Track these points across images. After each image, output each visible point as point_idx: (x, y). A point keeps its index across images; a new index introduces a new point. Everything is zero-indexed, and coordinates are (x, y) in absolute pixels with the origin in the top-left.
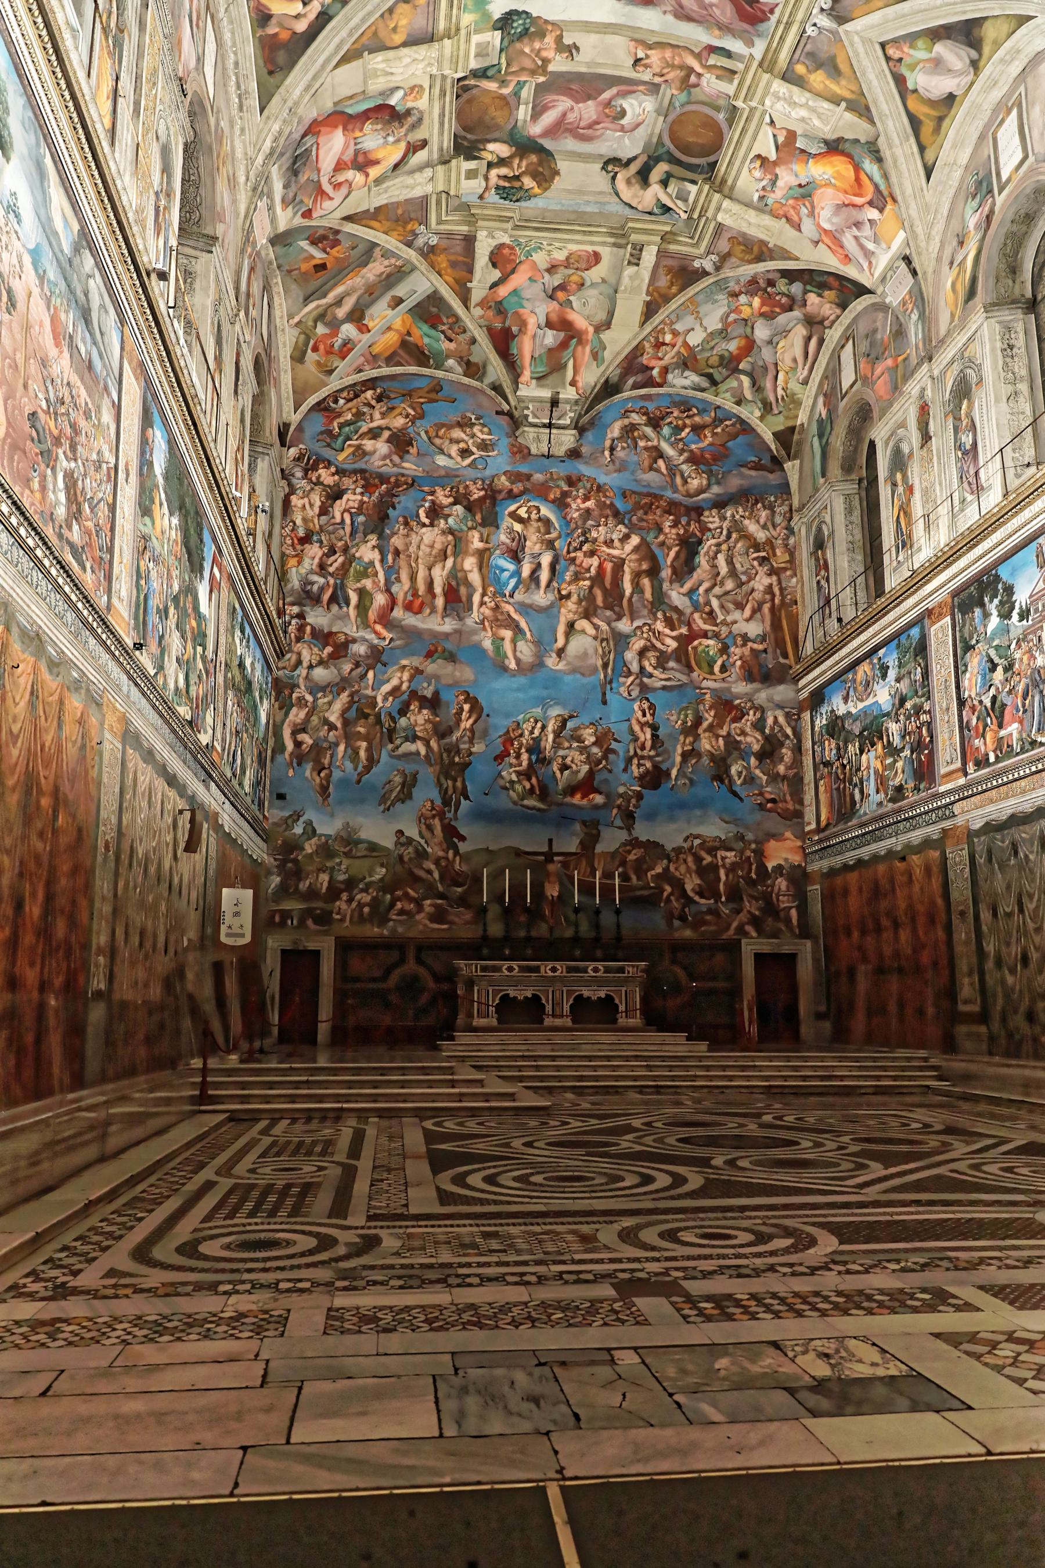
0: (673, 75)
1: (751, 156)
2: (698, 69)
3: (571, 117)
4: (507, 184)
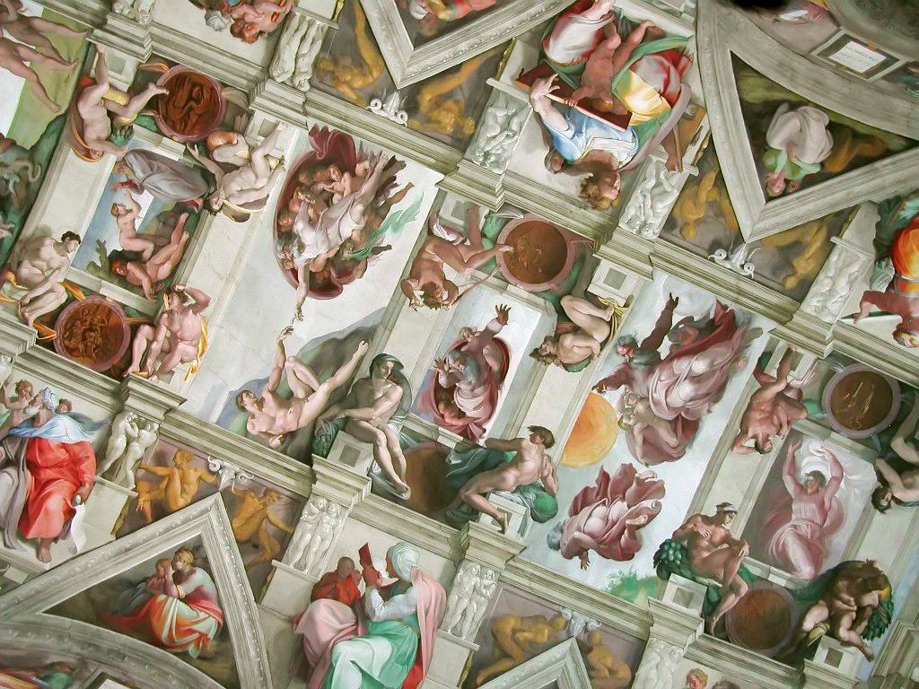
0: (782, 413)
1: (895, 343)
2: (781, 387)
3: (805, 530)
4: (865, 624)
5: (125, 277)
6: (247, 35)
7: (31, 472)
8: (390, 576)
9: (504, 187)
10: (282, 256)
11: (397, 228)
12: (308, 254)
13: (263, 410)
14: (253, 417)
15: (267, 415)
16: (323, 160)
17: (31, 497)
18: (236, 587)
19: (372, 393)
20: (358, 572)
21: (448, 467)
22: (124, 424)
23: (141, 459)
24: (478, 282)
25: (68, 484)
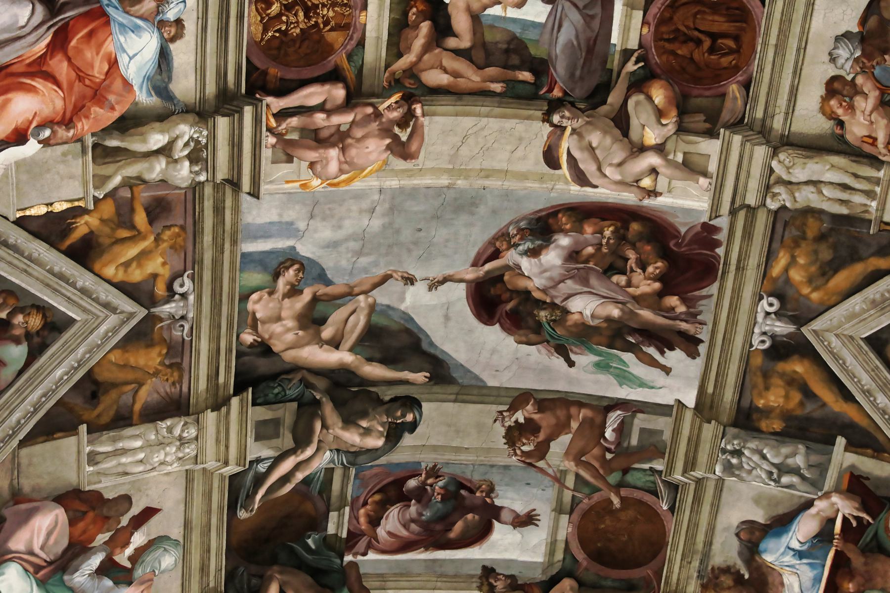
5: (407, 25)
6: (833, 102)
7: (51, 42)
8: (130, 559)
9: (699, 482)
10: (512, 231)
11: (602, 367)
12: (526, 264)
13: (286, 300)
14: (271, 294)
15: (281, 309)
16: (672, 251)
17: (15, 67)
18: (27, 406)
19: (364, 415)
20: (119, 523)
21: (300, 538)
22: (185, 131)
23: (144, 182)
24: (559, 479)
25: (59, 104)
